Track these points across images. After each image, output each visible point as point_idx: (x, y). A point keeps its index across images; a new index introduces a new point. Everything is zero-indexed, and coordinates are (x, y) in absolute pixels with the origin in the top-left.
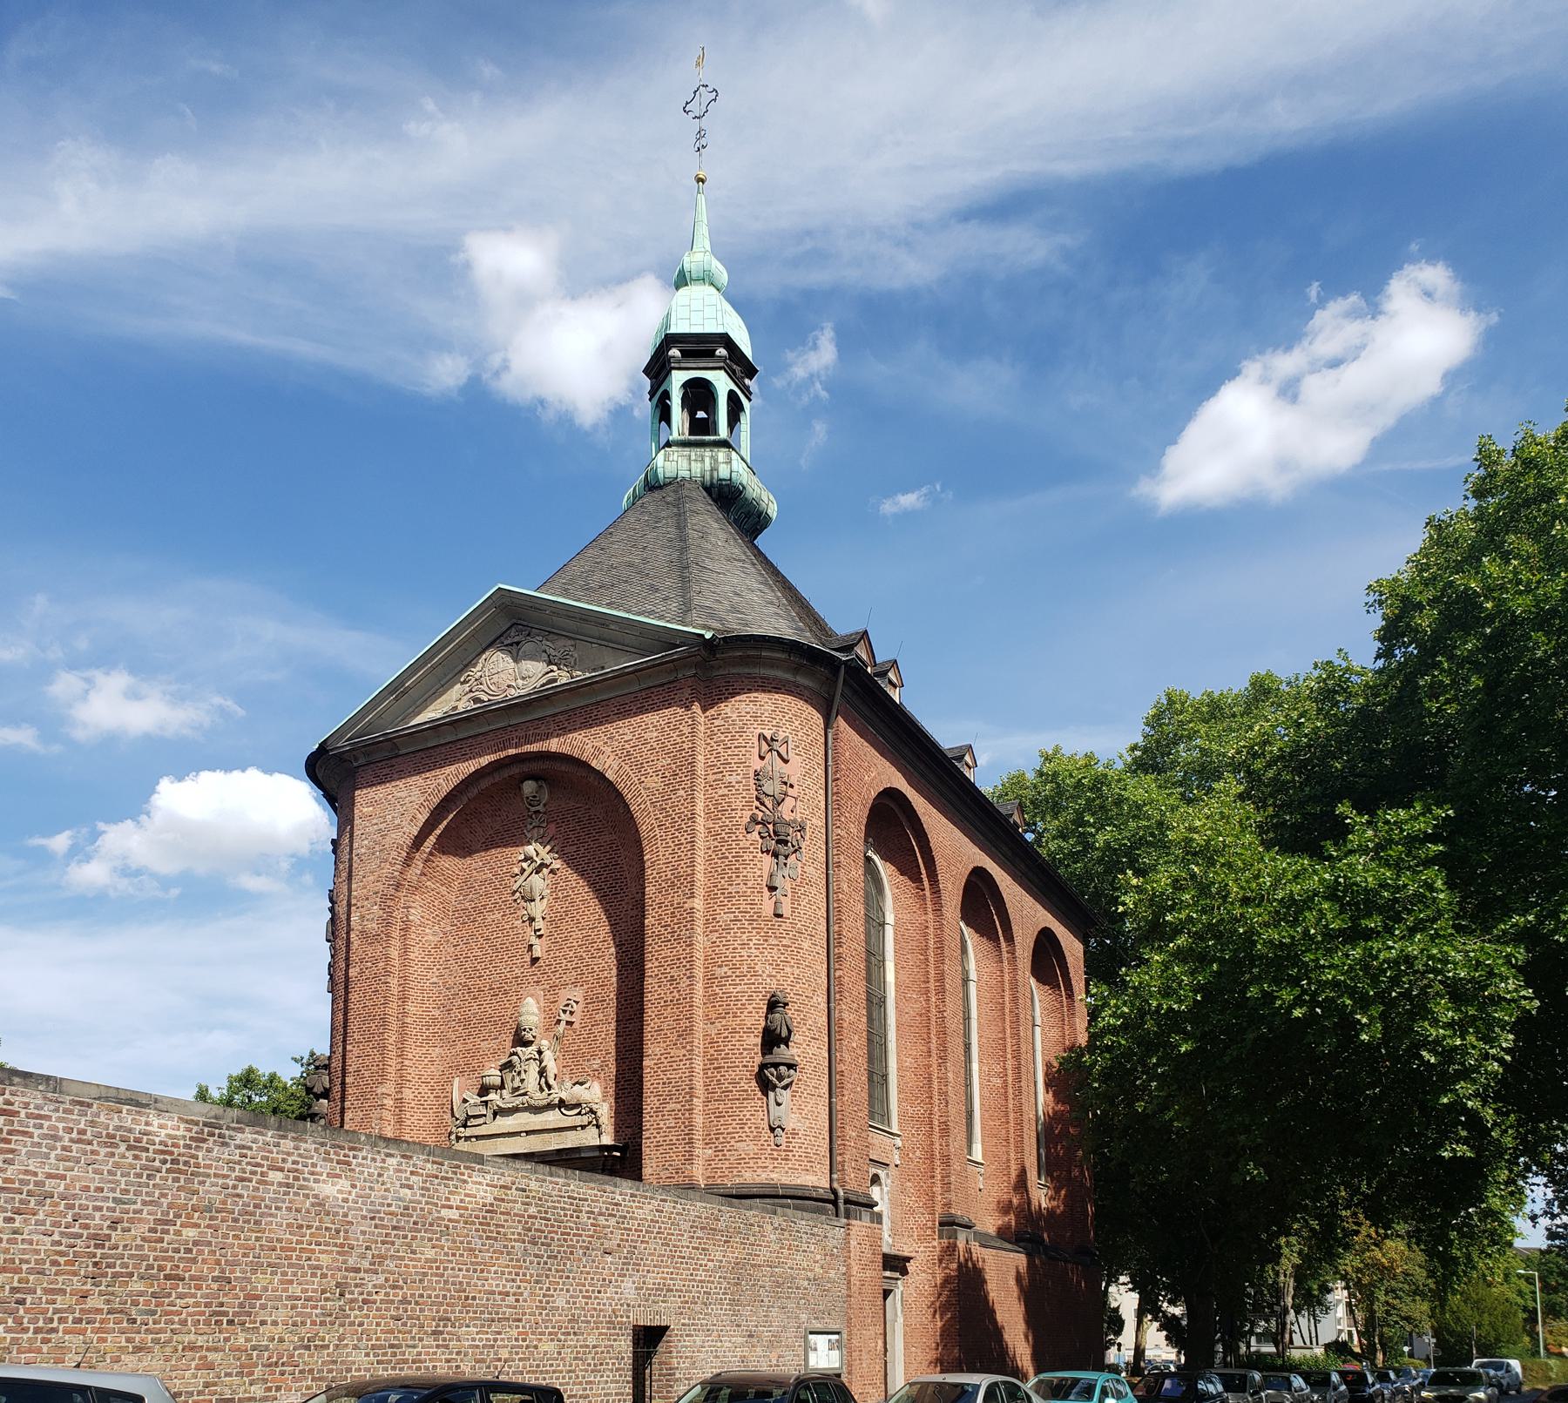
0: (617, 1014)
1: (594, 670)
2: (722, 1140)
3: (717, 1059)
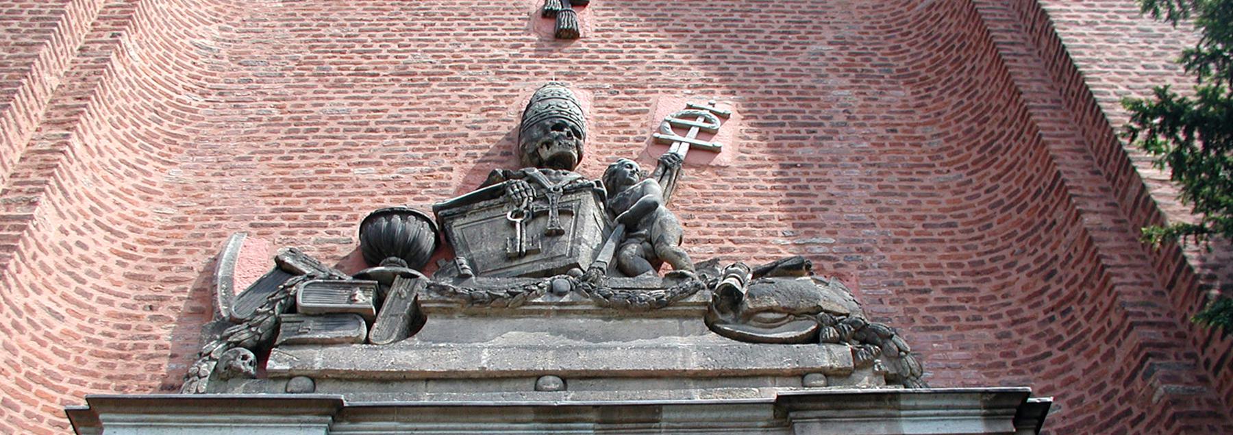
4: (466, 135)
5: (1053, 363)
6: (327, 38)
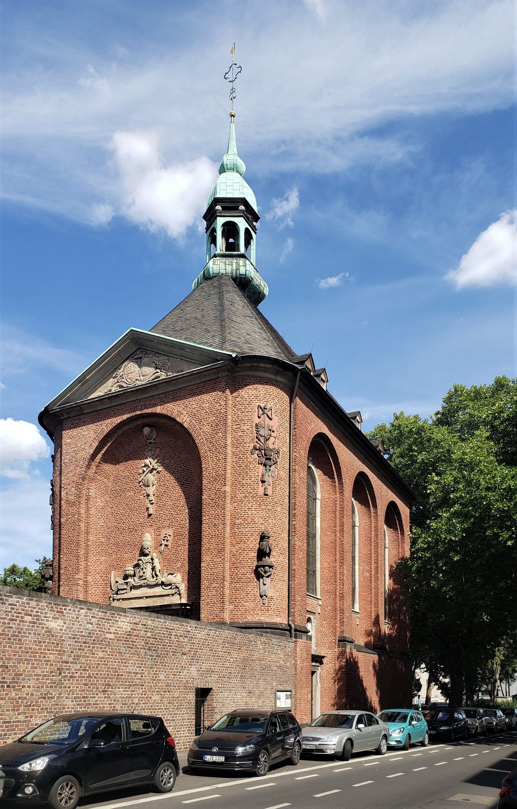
0: (189, 541)
1: (178, 372)
2: (238, 601)
3: (236, 563)
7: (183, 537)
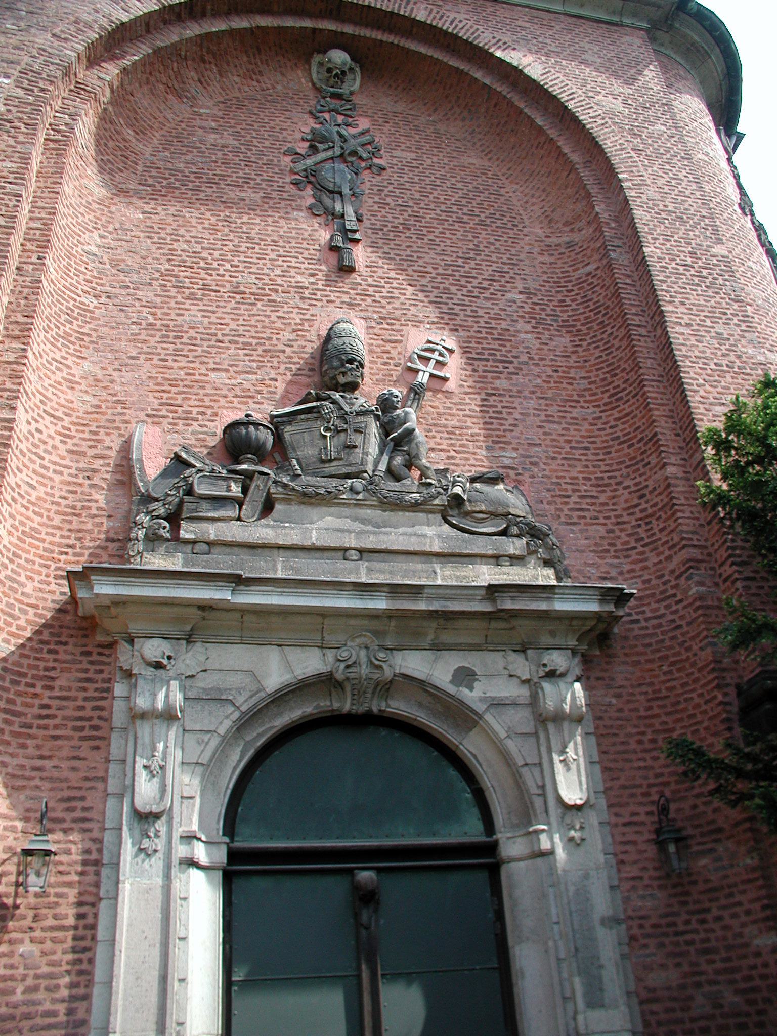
4: (284, 351)
5: (638, 554)
6: (179, 253)
7: (511, 370)
